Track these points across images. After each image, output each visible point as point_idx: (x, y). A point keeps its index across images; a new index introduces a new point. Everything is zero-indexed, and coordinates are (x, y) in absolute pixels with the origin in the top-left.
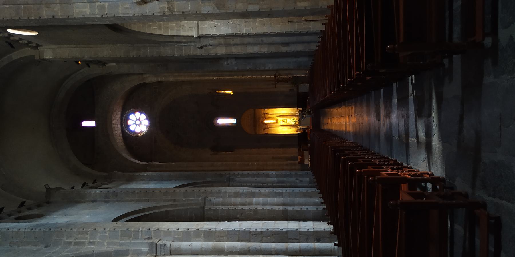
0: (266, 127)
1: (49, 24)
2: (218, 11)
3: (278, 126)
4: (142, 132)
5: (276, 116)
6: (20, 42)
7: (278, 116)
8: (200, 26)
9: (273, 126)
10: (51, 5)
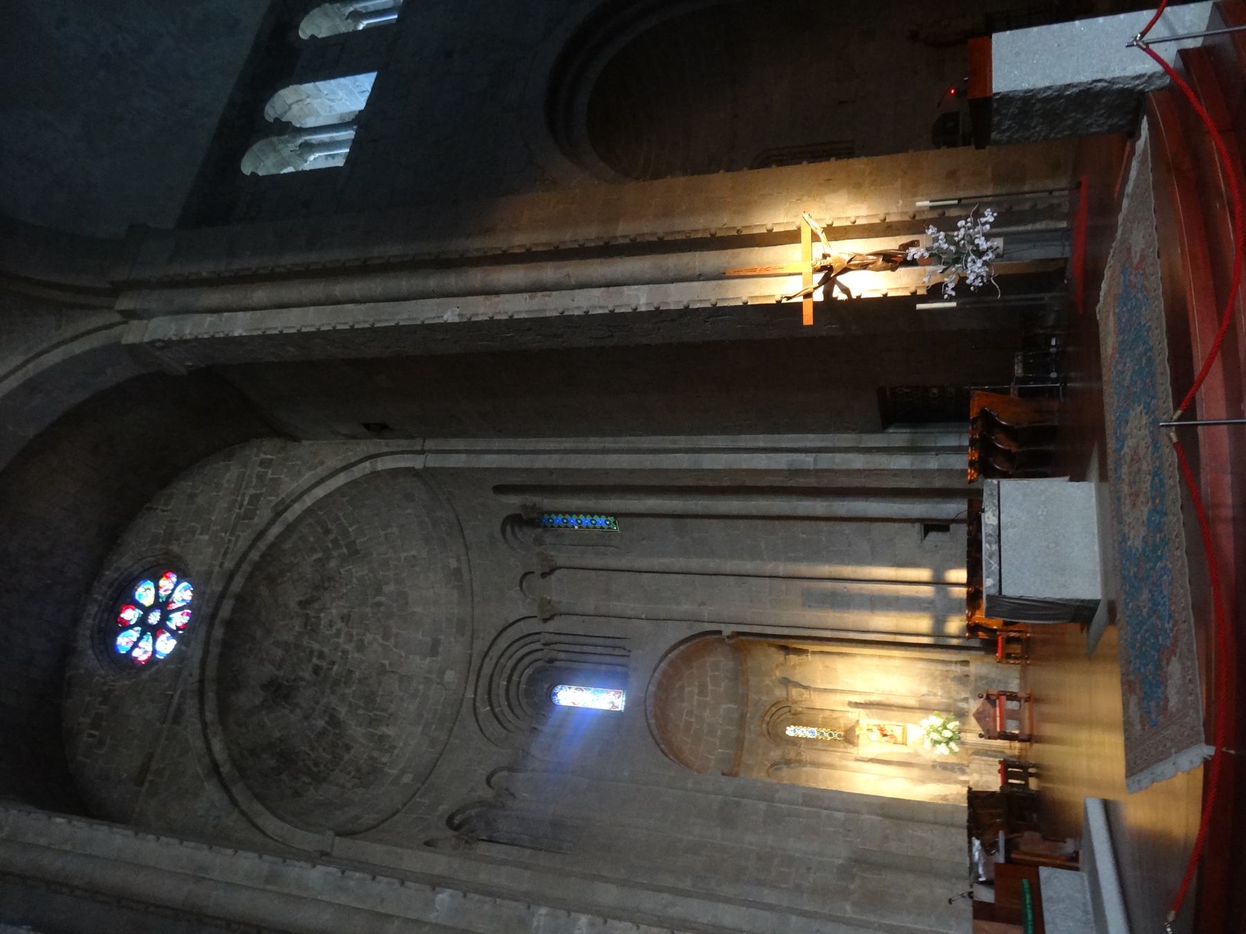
3: (857, 760)
5: (851, 704)
7: (857, 705)
9: (826, 758)
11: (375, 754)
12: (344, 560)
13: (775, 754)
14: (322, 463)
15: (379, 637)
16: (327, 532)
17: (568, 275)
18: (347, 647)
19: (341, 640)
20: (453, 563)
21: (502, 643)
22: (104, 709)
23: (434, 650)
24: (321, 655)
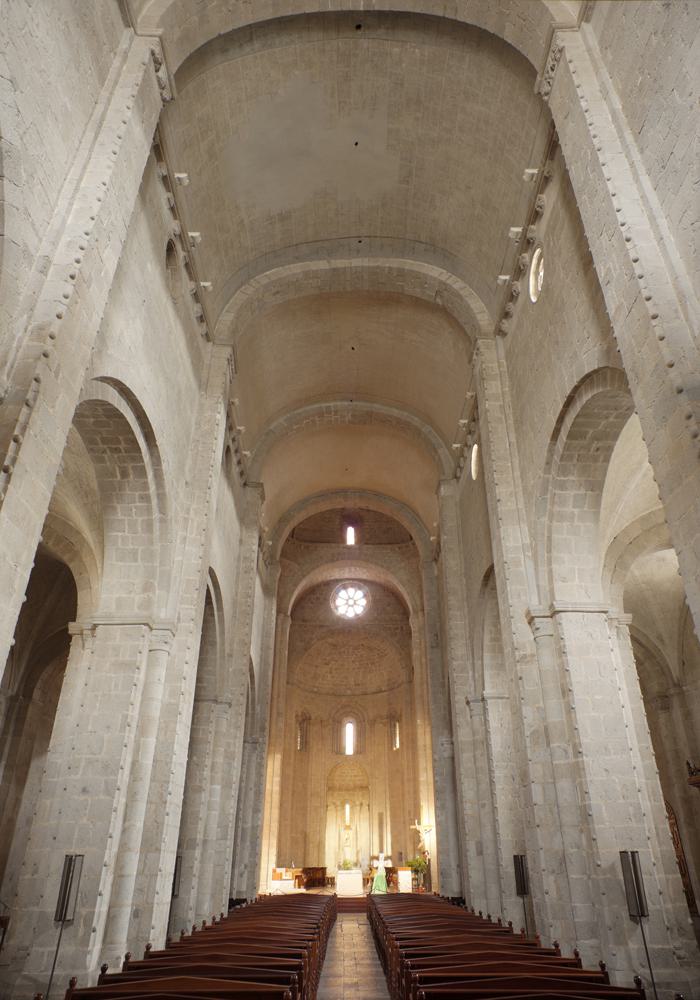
0: (339, 808)
1: (489, 495)
2: (527, 733)
4: (336, 608)
6: (462, 459)
8: (500, 701)
9: (339, 820)
10: (514, 499)
13: (338, 803)
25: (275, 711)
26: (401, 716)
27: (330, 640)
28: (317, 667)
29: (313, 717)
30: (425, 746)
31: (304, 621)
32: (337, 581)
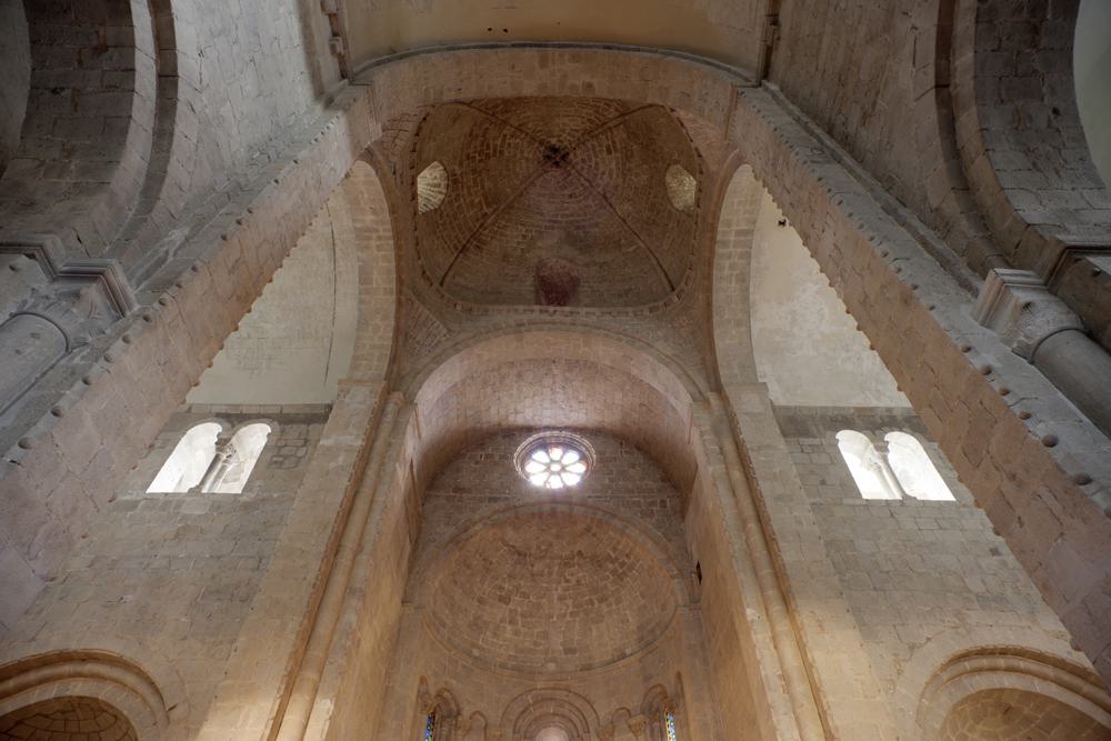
4: (528, 476)
11: (491, 627)
12: (614, 572)
14: (669, 540)
15: (571, 609)
16: (627, 556)
17: (802, 706)
18: (560, 589)
19: (564, 585)
20: (628, 651)
21: (578, 703)
22: (497, 458)
23: (569, 651)
24: (550, 574)
25: (339, 579)
26: (681, 694)
27: (510, 534)
28: (481, 601)
29: (466, 712)
30: (785, 677)
31: (458, 489)
32: (529, 430)
